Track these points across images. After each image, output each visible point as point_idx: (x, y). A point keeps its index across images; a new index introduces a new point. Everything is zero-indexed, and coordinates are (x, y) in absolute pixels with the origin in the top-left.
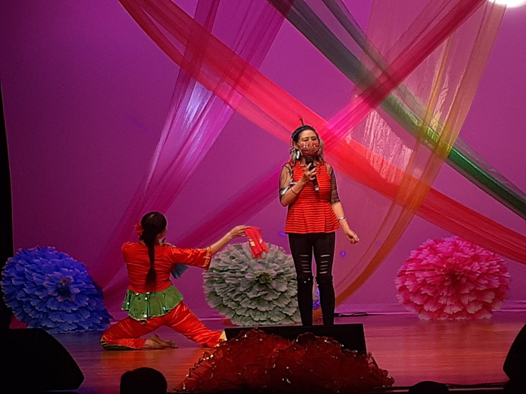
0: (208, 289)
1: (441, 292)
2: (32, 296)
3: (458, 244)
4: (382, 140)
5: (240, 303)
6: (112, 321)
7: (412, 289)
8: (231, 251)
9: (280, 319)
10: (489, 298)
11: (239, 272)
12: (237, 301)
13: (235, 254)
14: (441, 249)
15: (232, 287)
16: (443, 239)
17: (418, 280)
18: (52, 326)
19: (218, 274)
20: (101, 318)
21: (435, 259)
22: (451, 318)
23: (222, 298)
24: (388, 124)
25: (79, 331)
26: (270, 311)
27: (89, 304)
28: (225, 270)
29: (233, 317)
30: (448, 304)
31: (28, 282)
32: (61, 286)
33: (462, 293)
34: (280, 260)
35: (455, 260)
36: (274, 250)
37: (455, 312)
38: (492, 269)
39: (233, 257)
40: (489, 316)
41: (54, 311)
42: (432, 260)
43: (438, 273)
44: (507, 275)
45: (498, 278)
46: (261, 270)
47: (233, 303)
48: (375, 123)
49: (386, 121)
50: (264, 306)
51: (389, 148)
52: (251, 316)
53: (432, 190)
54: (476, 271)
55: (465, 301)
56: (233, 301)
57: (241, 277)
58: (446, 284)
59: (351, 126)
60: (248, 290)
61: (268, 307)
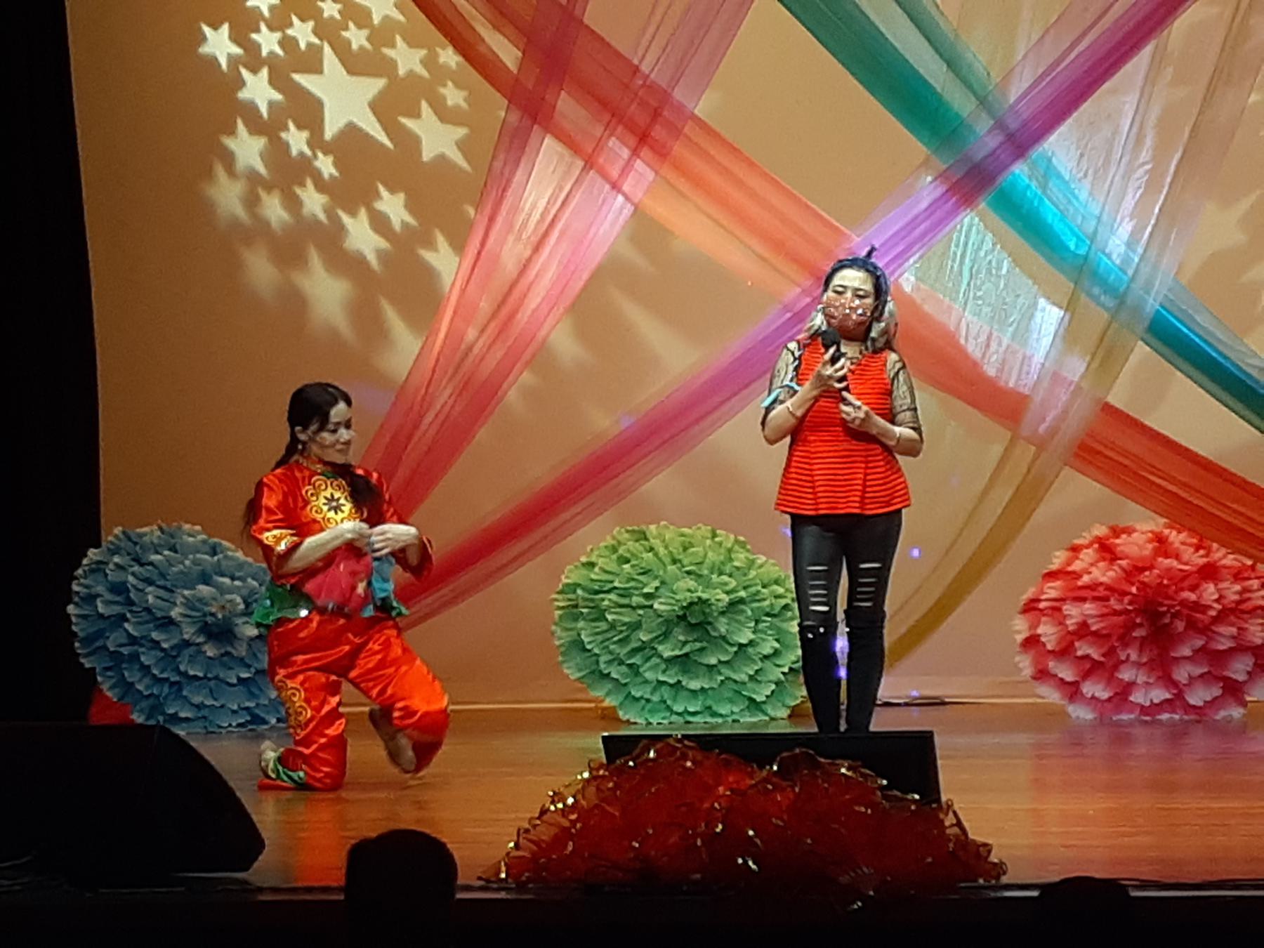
3: (1167, 537)
5: (641, 670)
8: (620, 543)
9: (736, 709)
11: (637, 595)
12: (634, 664)
13: (629, 551)
15: (621, 632)
18: (189, 715)
19: (587, 600)
21: (1111, 574)
22: (1148, 715)
26: (712, 689)
28: (605, 589)
29: (621, 704)
30: (1139, 681)
31: (134, 609)
32: (213, 619)
33: (1173, 654)
34: (738, 568)
35: (1159, 576)
37: (1156, 701)
38: (1249, 599)
39: (626, 558)
40: (1237, 712)
41: (195, 677)
42: (1104, 575)
43: (1118, 607)
46: (689, 590)
47: (624, 669)
48: (973, 244)
50: (697, 677)
51: (1006, 304)
52: (665, 702)
53: (1108, 409)
54: (1209, 603)
56: (621, 663)
58: (1134, 634)
59: (915, 249)
61: (707, 681)
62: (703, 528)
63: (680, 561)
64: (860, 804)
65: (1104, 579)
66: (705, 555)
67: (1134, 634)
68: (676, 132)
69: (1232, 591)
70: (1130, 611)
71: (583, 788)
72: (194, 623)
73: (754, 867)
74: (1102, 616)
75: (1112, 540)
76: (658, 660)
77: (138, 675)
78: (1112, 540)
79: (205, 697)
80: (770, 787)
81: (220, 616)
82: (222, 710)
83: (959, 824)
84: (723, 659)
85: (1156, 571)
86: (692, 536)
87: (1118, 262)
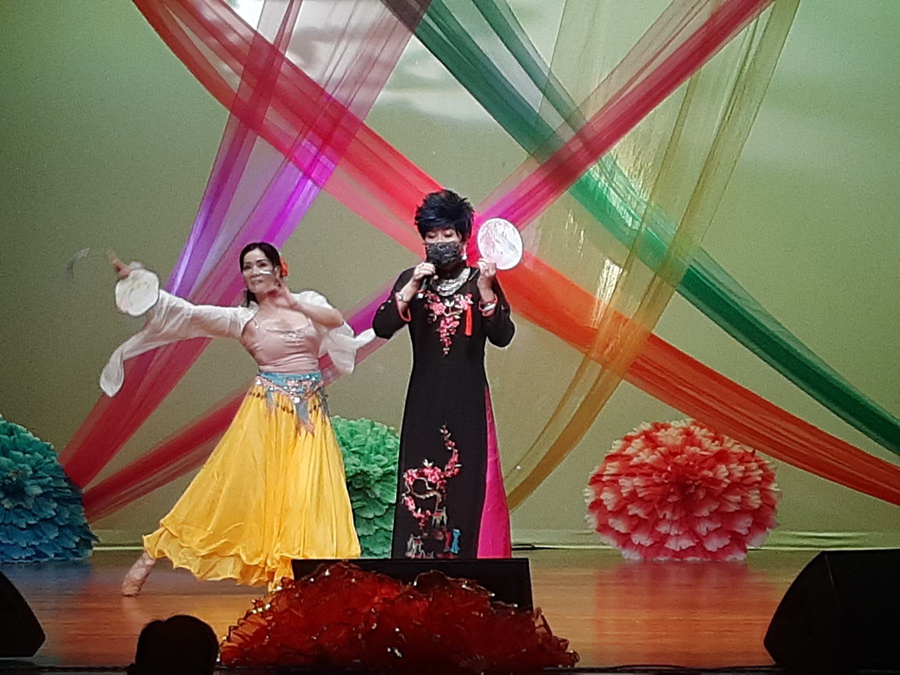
1: (662, 512)
6: (97, 546)
7: (612, 506)
14: (664, 440)
16: (667, 422)
20: (77, 539)
21: (653, 457)
22: (677, 557)
25: (38, 560)
26: (369, 535)
27: (57, 515)
30: (672, 534)
34: (389, 450)
36: (380, 433)
37: (684, 548)
38: (749, 476)
40: (740, 557)
42: (648, 457)
43: (657, 481)
44: (773, 487)
46: (355, 465)
53: (653, 339)
58: (669, 500)
62: (365, 421)
63: (348, 444)
65: (648, 461)
66: (366, 440)
67: (669, 500)
68: (351, 135)
69: (738, 470)
70: (667, 484)
74: (644, 487)
75: (654, 434)
78: (654, 434)
81: (14, 479)
82: (15, 547)
84: (378, 514)
85: (684, 456)
86: (356, 426)
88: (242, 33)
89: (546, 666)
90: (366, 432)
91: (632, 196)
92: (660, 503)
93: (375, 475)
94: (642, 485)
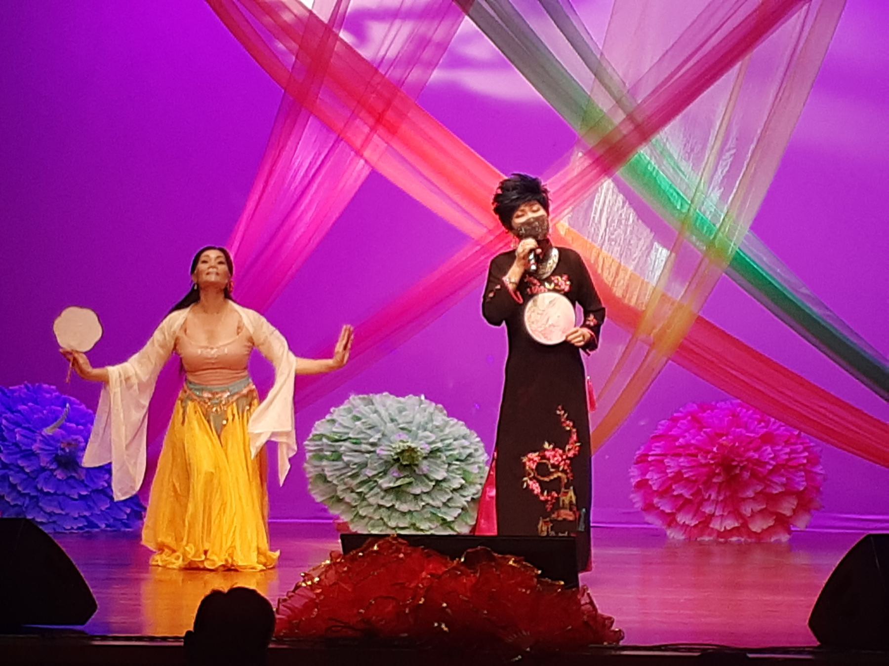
0: (312, 470)
2: (11, 467)
4: (619, 230)
8: (354, 407)
9: (433, 526)
10: (787, 508)
11: (365, 444)
12: (361, 492)
13: (359, 412)
15: (354, 469)
17: (668, 471)
18: (44, 520)
19: (330, 445)
20: (128, 511)
22: (722, 538)
23: (337, 486)
24: (630, 204)
28: (342, 438)
29: (352, 520)
30: (717, 514)
31: (7, 443)
32: (63, 453)
34: (437, 427)
35: (734, 441)
37: (728, 528)
38: (795, 458)
39: (357, 417)
40: (785, 538)
41: (48, 494)
42: (693, 438)
43: (703, 461)
44: (819, 469)
45: (803, 474)
46: (402, 441)
47: (354, 495)
49: (627, 198)
50: (406, 502)
52: (382, 519)
54: (767, 460)
55: (747, 510)
56: (352, 491)
57: (369, 452)
58: (715, 480)
59: (569, 203)
60: (381, 475)
61: (413, 505)
63: (396, 420)
64: (523, 588)
65: (693, 442)
66: (414, 417)
68: (402, 116)
70: (712, 464)
71: (326, 571)
72: (49, 454)
73: (446, 629)
76: (379, 490)
77: (8, 490)
79: (55, 507)
80: (459, 573)
83: (591, 603)
84: (425, 491)
87: (709, 218)
88: (295, 11)
89: (592, 643)
90: (414, 409)
91: (681, 179)
92: (704, 483)
93: (422, 451)
94: (687, 465)
